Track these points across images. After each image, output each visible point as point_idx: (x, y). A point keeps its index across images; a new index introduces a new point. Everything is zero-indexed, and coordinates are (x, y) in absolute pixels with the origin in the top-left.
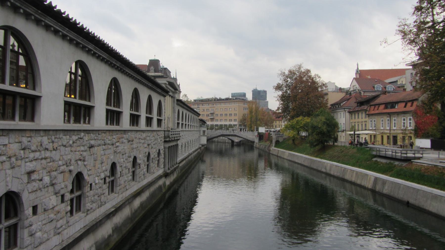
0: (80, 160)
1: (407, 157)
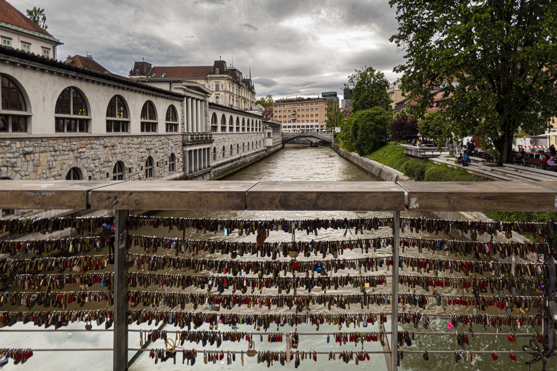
0: (7, 166)
1: (425, 155)
